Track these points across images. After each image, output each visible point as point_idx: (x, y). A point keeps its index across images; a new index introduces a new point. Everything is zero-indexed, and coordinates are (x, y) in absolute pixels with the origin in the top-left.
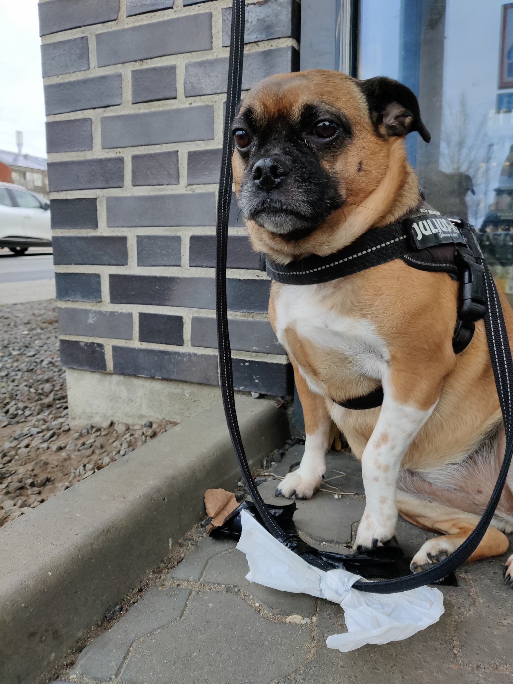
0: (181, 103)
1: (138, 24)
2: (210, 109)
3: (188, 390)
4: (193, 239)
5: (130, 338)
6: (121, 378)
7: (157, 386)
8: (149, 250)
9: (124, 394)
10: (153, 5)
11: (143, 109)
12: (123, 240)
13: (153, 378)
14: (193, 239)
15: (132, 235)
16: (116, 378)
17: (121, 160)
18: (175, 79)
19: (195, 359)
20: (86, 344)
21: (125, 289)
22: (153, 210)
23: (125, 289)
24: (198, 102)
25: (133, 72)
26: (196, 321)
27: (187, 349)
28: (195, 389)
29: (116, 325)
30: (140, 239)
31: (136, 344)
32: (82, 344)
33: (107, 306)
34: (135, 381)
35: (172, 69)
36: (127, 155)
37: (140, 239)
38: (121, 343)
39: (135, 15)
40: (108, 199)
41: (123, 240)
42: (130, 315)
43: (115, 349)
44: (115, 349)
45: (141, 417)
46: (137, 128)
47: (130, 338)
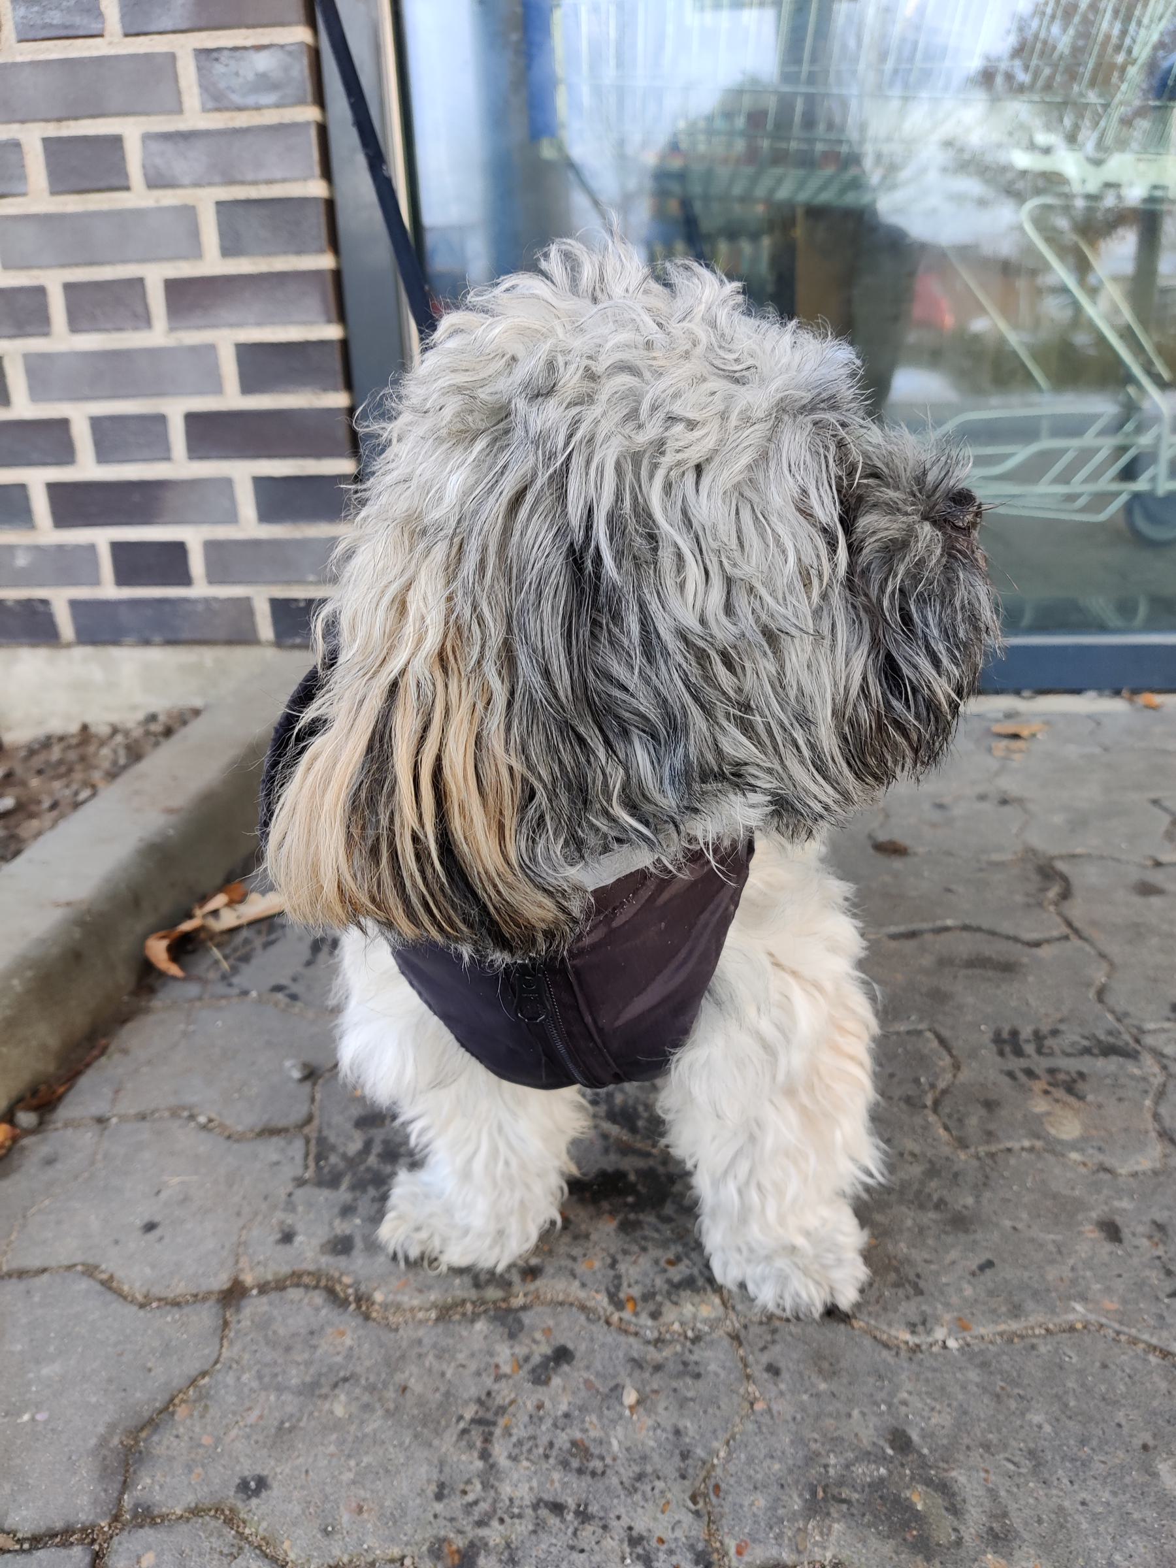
0: (138, 197)
1: (42, 57)
2: (189, 213)
3: (208, 656)
4: (192, 419)
5: (96, 582)
6: (88, 650)
7: (155, 654)
8: (112, 437)
9: (97, 674)
10: (66, 27)
11: (72, 204)
12: (63, 424)
13: (146, 643)
14: (192, 419)
15: (79, 415)
16: (80, 652)
17: (41, 291)
18: (123, 158)
19: (216, 606)
20: (19, 602)
21: (73, 504)
22: (113, 372)
23: (73, 504)
24: (169, 198)
25: (45, 140)
26: (211, 547)
27: (200, 589)
28: (221, 652)
29: (70, 565)
30: (97, 424)
31: (109, 590)
32: (9, 604)
33: (46, 532)
34: (115, 652)
35: (116, 142)
36: (54, 281)
37: (97, 424)
38: (83, 593)
39: (35, 40)
40: (27, 357)
41: (63, 424)
42: (92, 548)
43: (74, 604)
44: (74, 604)
45: (134, 708)
46: (66, 237)
47: (96, 582)
